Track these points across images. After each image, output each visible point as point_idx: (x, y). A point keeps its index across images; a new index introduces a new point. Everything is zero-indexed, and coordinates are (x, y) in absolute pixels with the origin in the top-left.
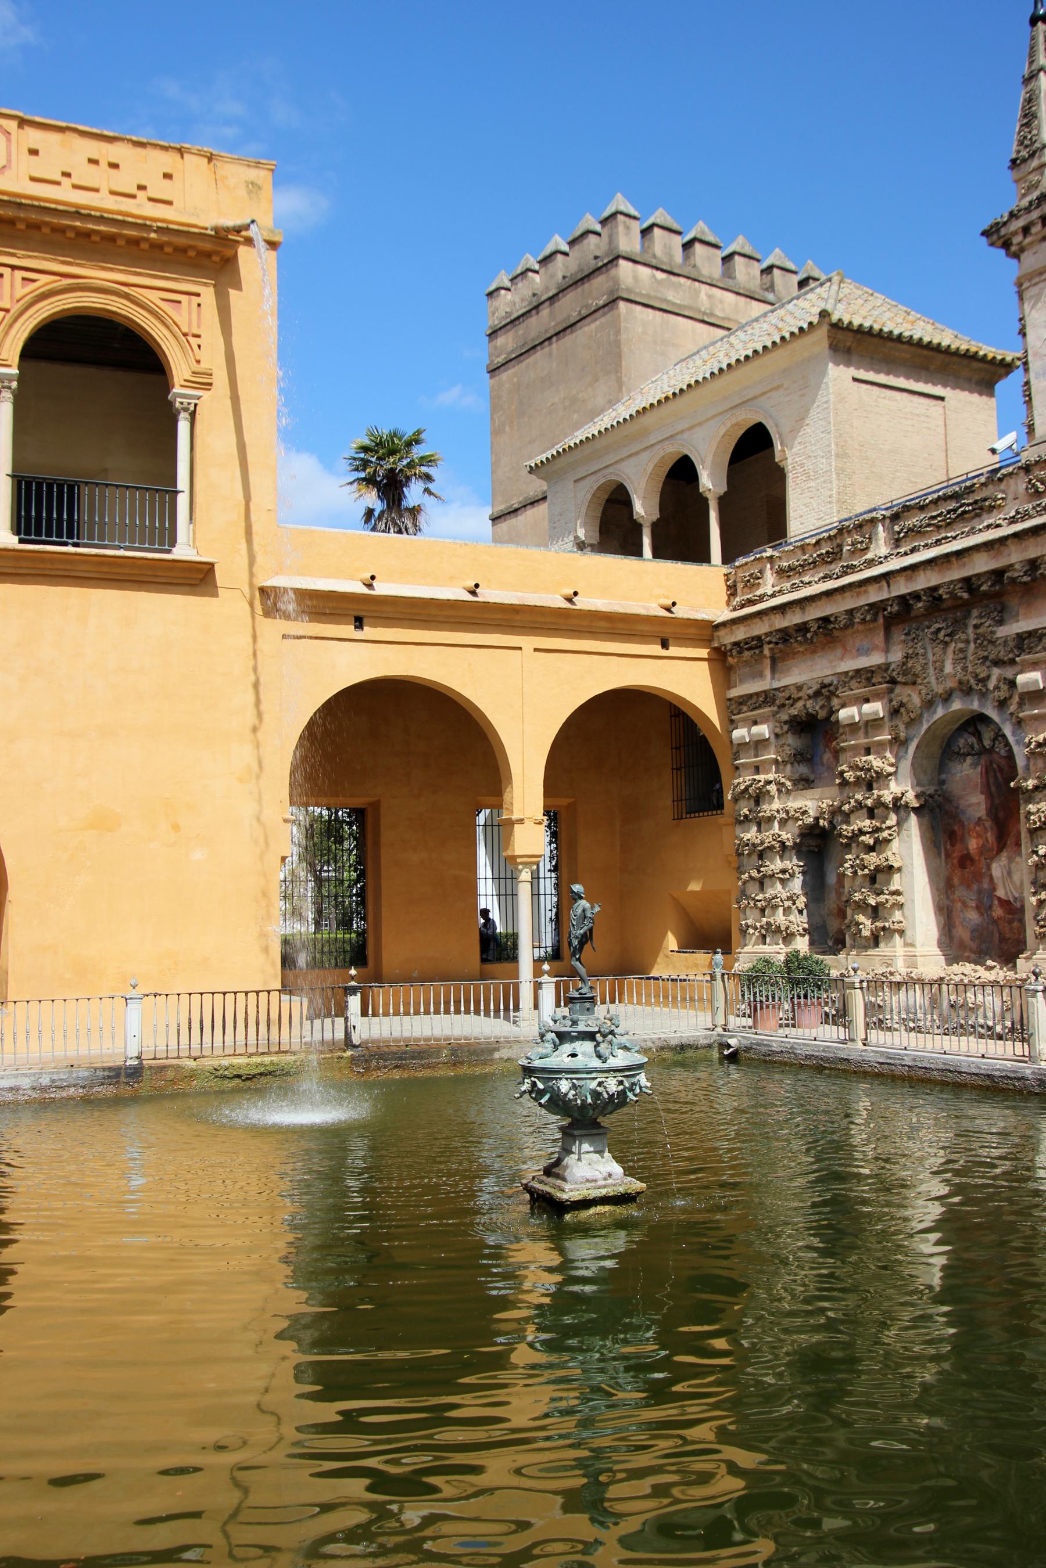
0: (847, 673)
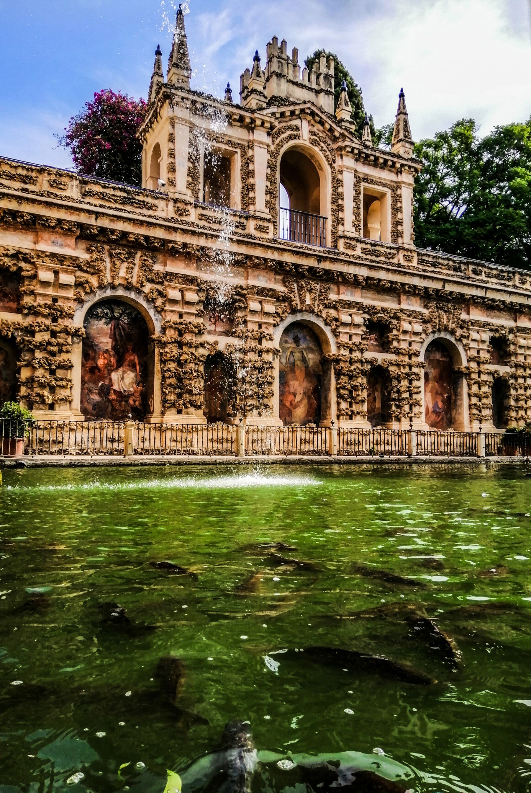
0: (43, 252)
